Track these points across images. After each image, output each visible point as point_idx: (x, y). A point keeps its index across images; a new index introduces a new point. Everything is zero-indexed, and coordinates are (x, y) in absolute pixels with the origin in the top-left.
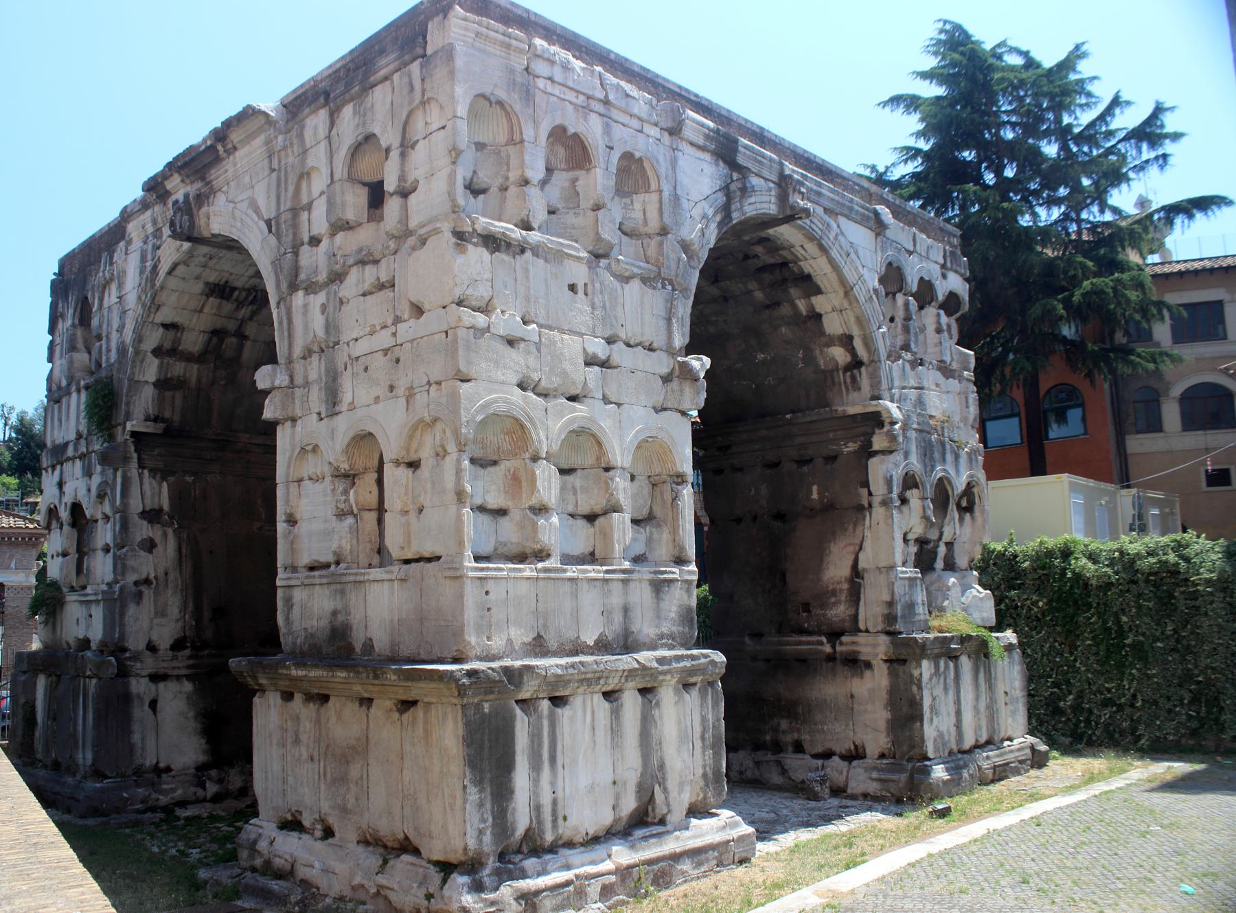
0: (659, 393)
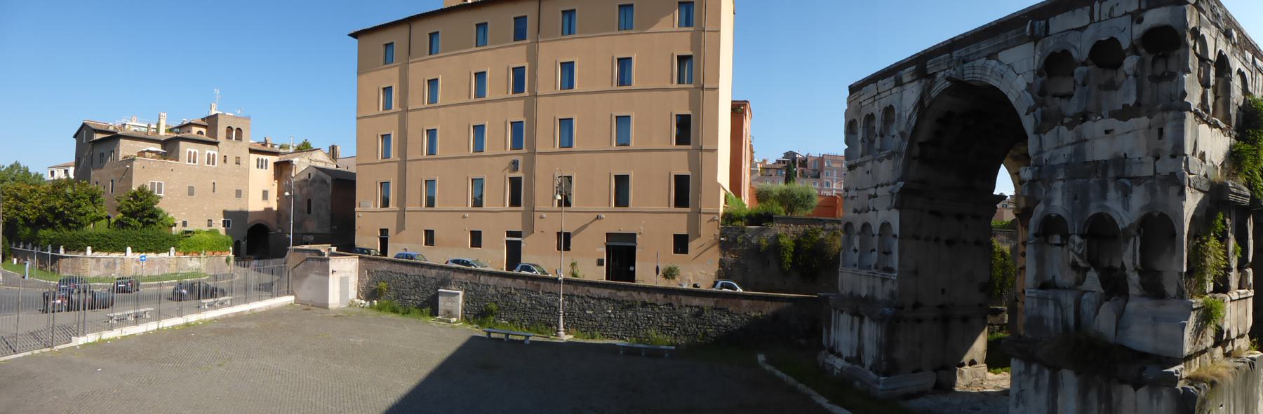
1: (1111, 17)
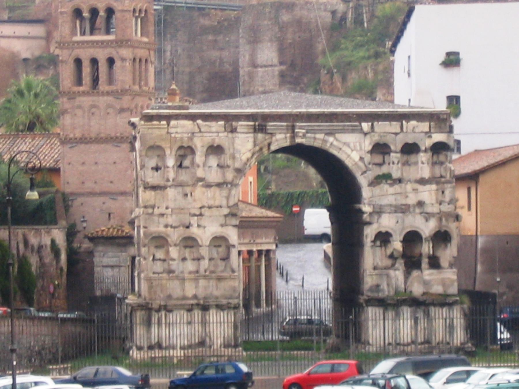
0: (222, 220)
1: (413, 132)
